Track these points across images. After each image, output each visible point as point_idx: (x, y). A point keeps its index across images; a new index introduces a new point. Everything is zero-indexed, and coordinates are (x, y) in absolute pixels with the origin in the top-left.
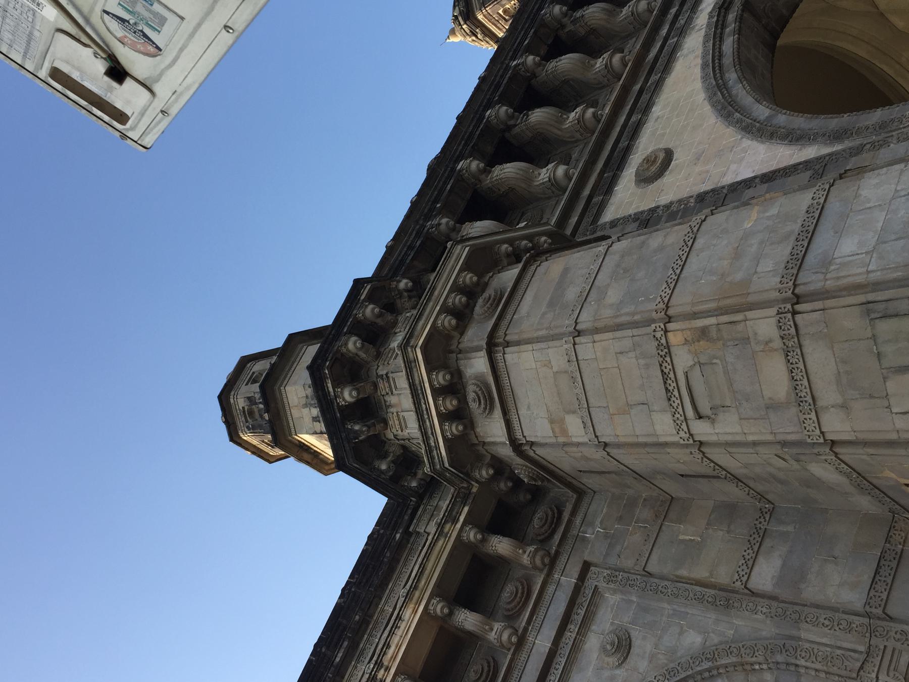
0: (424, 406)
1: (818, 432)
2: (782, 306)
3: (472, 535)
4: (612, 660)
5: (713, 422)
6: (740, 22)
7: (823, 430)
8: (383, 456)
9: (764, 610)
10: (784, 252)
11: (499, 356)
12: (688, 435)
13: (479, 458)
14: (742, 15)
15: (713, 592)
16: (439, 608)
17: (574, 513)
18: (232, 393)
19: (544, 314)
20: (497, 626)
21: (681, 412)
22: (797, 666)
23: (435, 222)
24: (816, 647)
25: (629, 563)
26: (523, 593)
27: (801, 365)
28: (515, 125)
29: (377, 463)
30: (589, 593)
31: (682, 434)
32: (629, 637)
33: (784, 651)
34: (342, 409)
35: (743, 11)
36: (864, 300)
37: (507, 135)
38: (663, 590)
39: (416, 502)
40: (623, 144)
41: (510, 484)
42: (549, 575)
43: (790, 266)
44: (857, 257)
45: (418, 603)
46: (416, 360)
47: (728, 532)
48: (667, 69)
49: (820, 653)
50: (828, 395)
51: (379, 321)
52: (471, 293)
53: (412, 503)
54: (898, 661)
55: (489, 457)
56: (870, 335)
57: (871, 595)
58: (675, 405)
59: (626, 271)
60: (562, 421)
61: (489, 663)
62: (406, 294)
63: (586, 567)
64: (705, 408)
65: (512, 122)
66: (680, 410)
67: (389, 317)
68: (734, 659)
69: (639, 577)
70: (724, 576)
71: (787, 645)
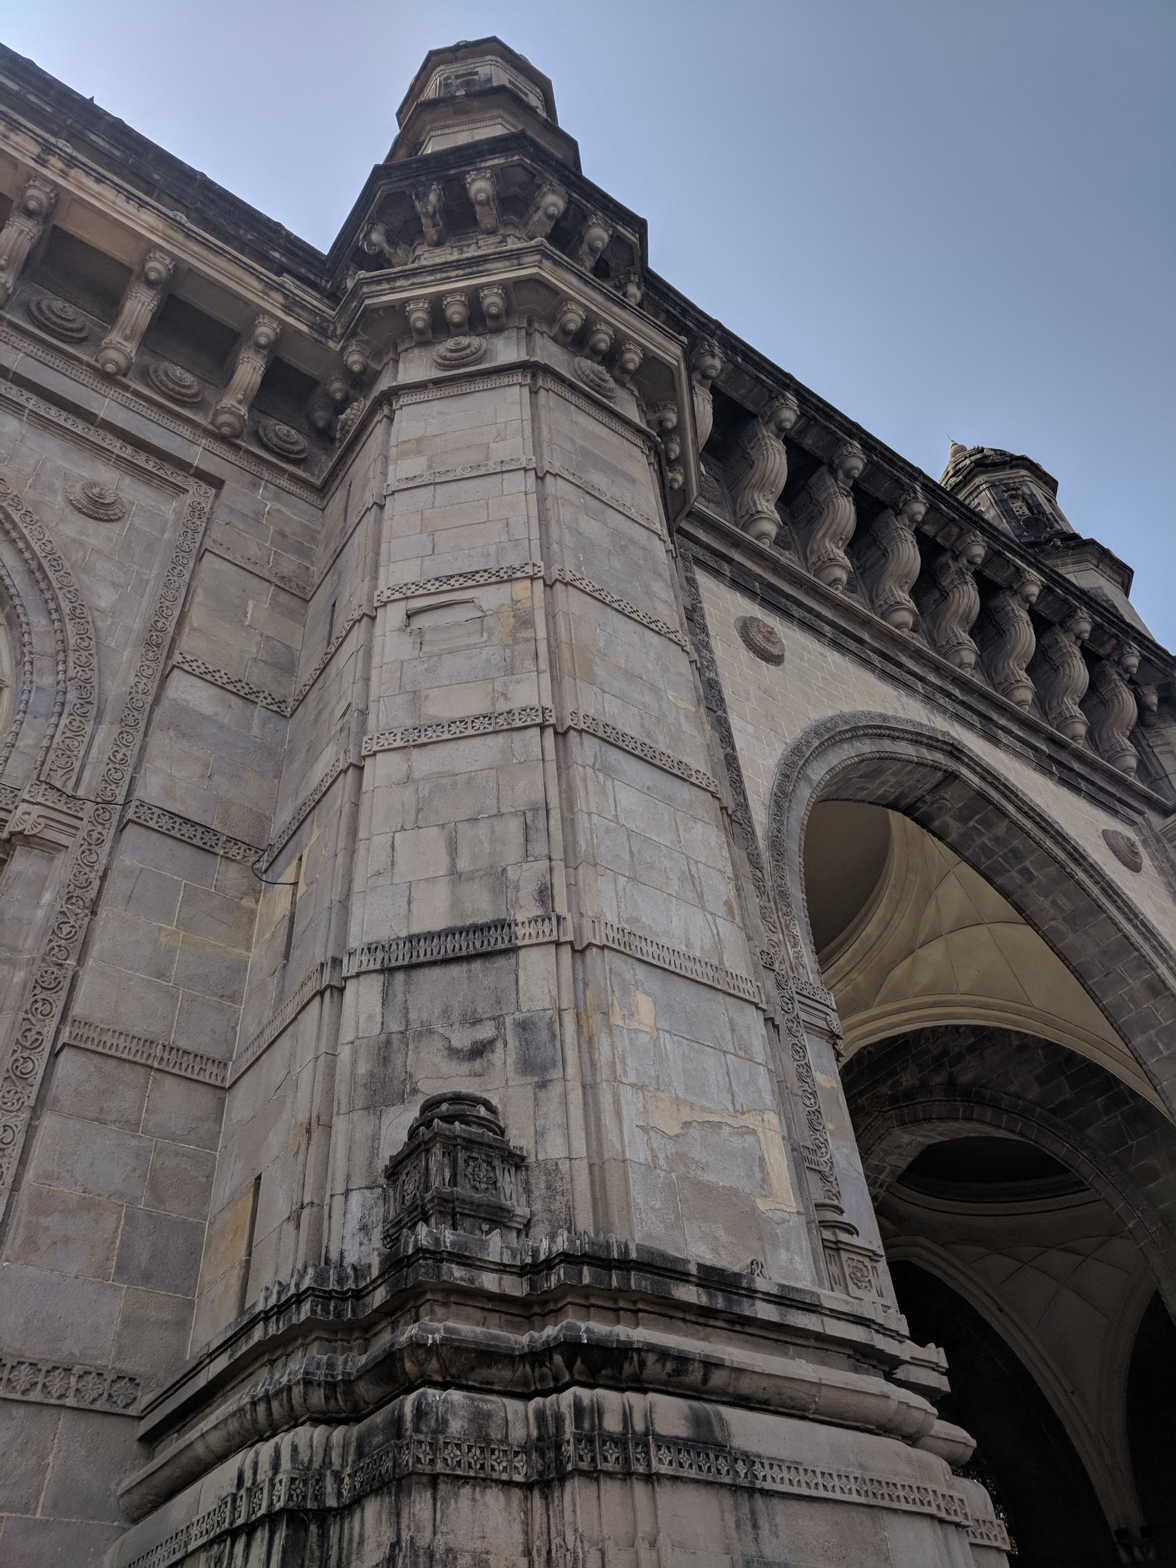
0: (454, 274)
1: (376, 748)
2: (553, 714)
3: (265, 331)
4: (77, 492)
5: (401, 630)
6: (932, 766)
7: (378, 755)
9: (141, 686)
11: (519, 378)
13: (377, 355)
14: (940, 769)
15: (171, 629)
16: (157, 267)
17: (294, 478)
18: (499, 59)
19: (573, 441)
20: (131, 347)
21: (417, 593)
22: (60, 715)
23: (717, 351)
24: (86, 740)
25: (217, 533)
26: (180, 393)
27: (470, 732)
28: (836, 479)
29: (380, 228)
30: (179, 480)
32: (111, 521)
34: (460, 178)
35: (945, 771)
36: (551, 806)
37: (824, 469)
39: (325, 289)
40: (796, 611)
41: (338, 396)
42: (207, 433)
43: (609, 730)
44: (612, 805)
45: (165, 238)
46: (521, 266)
47: (255, 659)
48: (885, 675)
49: (76, 744)
50: (424, 762)
51: (585, 248)
52: (611, 358)
53: (324, 283)
54: (61, 831)
55: (379, 369)
56: (503, 810)
57: (154, 809)
58: (428, 586)
59: (624, 548)
60: (419, 452)
61: (78, 330)
63: (217, 483)
64: (419, 622)
65: (841, 475)
66: (421, 591)
67: (590, 262)
69: (197, 545)
70: (189, 644)
71: (90, 706)
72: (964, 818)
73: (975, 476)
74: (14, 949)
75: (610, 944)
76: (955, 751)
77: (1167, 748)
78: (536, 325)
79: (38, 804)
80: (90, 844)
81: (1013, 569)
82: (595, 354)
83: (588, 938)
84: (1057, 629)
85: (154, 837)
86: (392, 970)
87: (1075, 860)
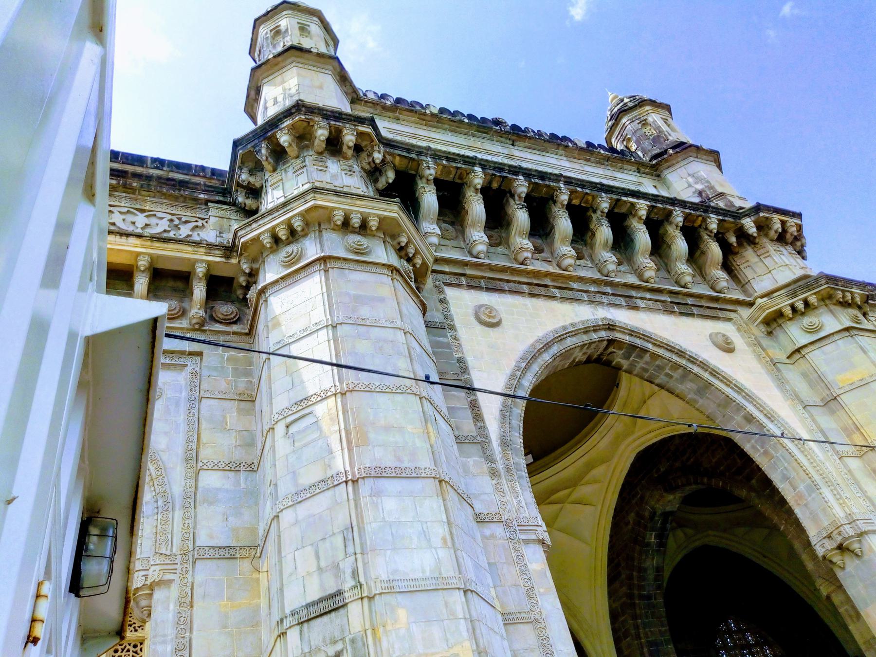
1: (282, 507)
2: (350, 473)
3: (200, 270)
5: (285, 436)
6: (598, 341)
7: (284, 511)
8: (251, 173)
9: (188, 484)
10: (389, 461)
11: (317, 267)
12: (276, 420)
13: (254, 260)
14: (604, 340)
15: (195, 448)
16: (143, 263)
18: (290, 12)
19: (348, 294)
21: (289, 413)
22: (157, 513)
23: (431, 164)
24: (170, 523)
25: (205, 386)
27: (318, 491)
28: (514, 201)
29: (245, 170)
31: (276, 416)
33: (165, 503)
35: (608, 340)
36: (353, 525)
38: (191, 414)
39: (230, 202)
40: (506, 286)
41: (244, 284)
43: (377, 469)
46: (306, 202)
47: (235, 446)
49: (167, 526)
50: (302, 511)
51: (345, 148)
52: (364, 227)
53: (229, 198)
54: (169, 574)
55: (258, 267)
57: (206, 548)
58: (293, 408)
59: (381, 348)
62: (371, 160)
64: (293, 429)
65: (517, 198)
66: (290, 412)
67: (350, 153)
68: (154, 474)
69: (198, 394)
70: (206, 453)
71: (168, 504)
72: (627, 357)
73: (621, 118)
74: (165, 636)
75: (384, 591)
76: (610, 327)
77: (747, 264)
78: (322, 227)
79: (157, 565)
80: (183, 575)
81: (629, 204)
82: (354, 231)
83: (374, 592)
84: (666, 223)
85: (208, 561)
86: (302, 623)
87: (692, 362)
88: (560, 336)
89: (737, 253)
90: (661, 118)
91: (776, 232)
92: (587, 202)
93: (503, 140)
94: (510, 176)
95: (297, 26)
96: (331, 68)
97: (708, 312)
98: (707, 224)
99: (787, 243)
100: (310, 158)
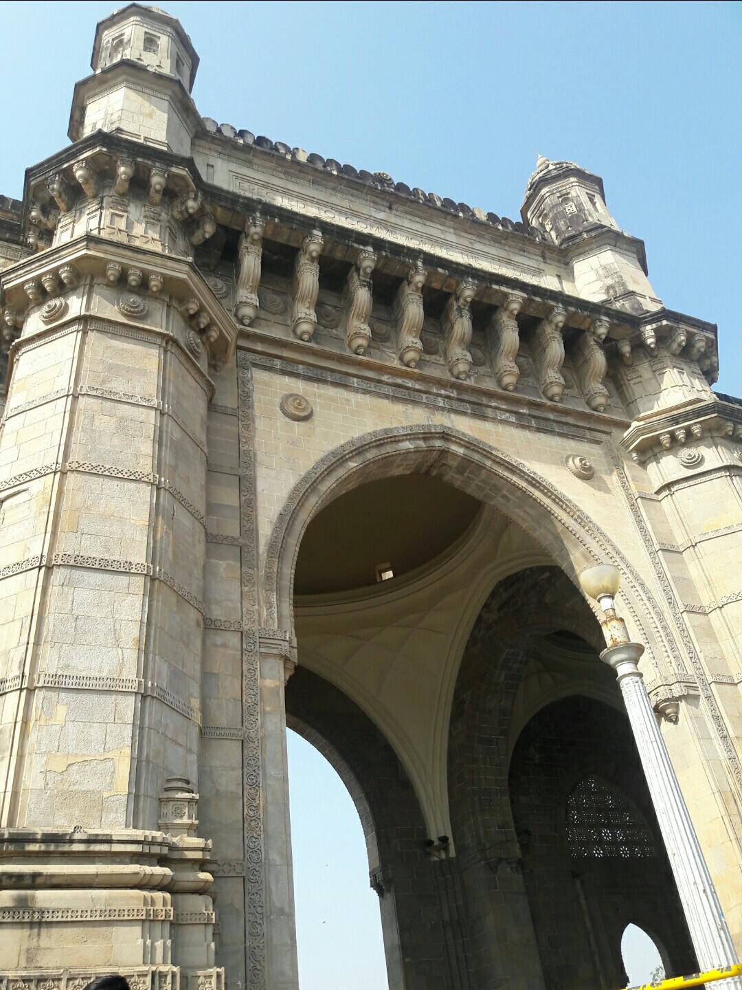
6: (427, 450)
18: (138, 18)
28: (359, 275)
43: (78, 558)
44: (70, 603)
51: (152, 190)
62: (184, 208)
65: (361, 272)
73: (540, 190)
75: (46, 685)
76: (445, 436)
77: (639, 379)
78: (95, 281)
82: (132, 290)
83: (36, 684)
84: (545, 322)
88: (379, 440)
89: (628, 366)
90: (587, 193)
91: (679, 345)
92: (449, 286)
93: (378, 200)
94: (356, 245)
95: (142, 37)
96: (170, 92)
97: (573, 431)
98: (595, 328)
99: (692, 361)
100: (109, 195)
